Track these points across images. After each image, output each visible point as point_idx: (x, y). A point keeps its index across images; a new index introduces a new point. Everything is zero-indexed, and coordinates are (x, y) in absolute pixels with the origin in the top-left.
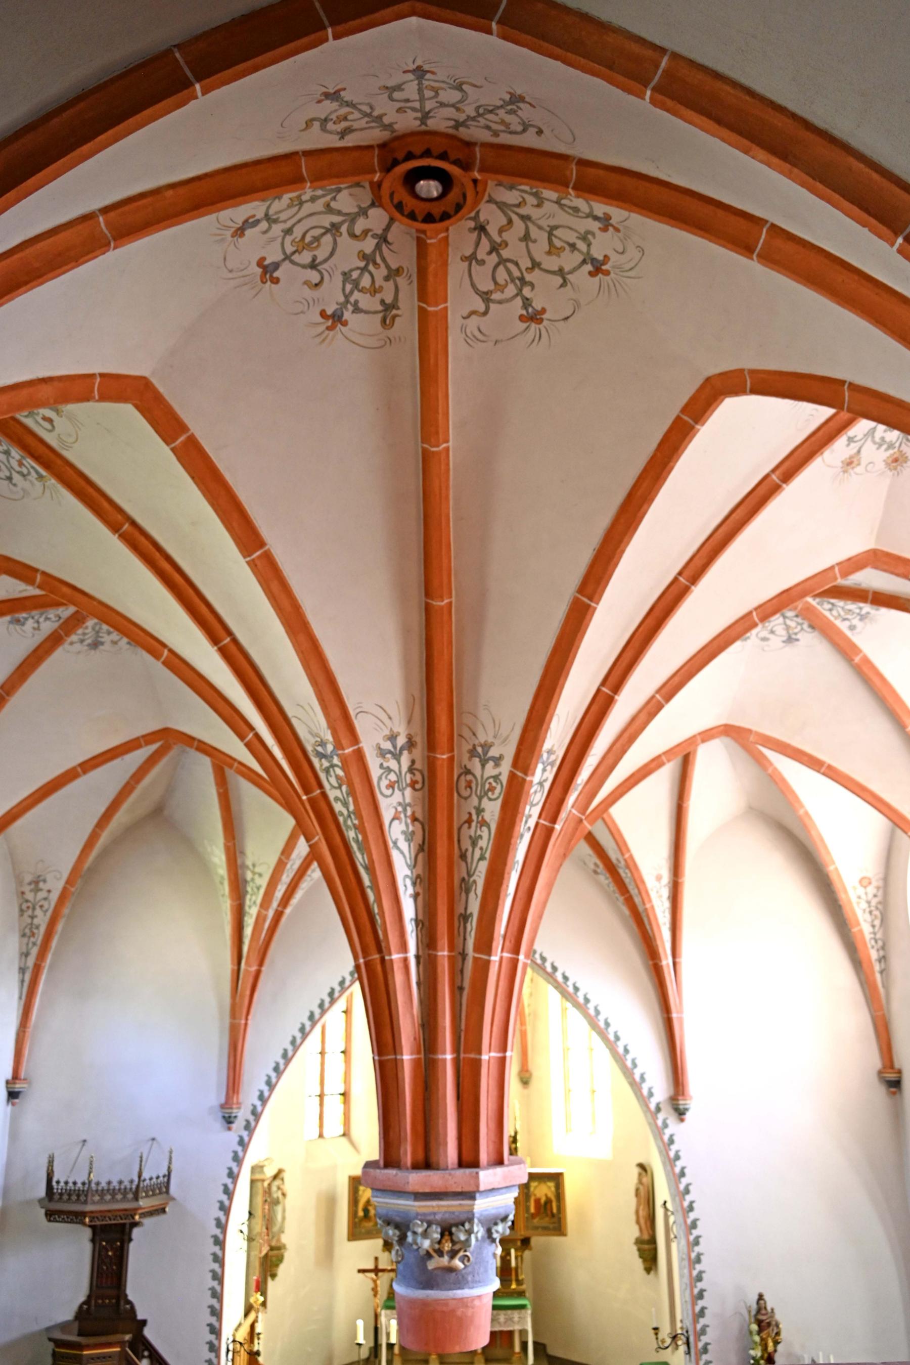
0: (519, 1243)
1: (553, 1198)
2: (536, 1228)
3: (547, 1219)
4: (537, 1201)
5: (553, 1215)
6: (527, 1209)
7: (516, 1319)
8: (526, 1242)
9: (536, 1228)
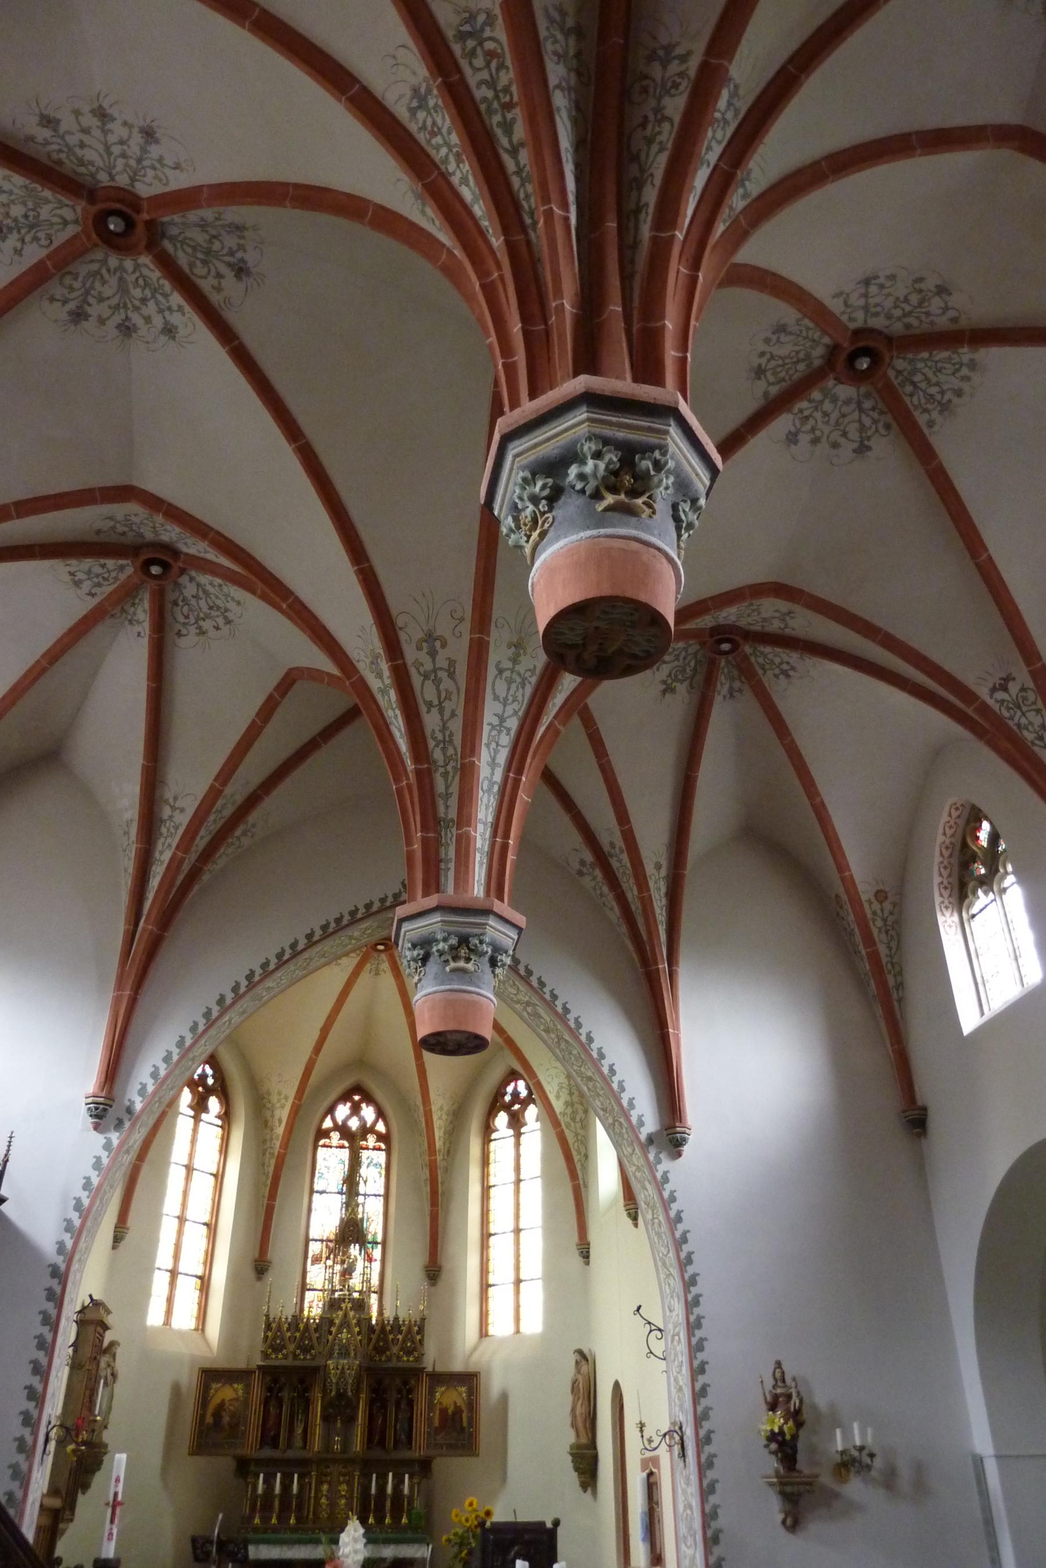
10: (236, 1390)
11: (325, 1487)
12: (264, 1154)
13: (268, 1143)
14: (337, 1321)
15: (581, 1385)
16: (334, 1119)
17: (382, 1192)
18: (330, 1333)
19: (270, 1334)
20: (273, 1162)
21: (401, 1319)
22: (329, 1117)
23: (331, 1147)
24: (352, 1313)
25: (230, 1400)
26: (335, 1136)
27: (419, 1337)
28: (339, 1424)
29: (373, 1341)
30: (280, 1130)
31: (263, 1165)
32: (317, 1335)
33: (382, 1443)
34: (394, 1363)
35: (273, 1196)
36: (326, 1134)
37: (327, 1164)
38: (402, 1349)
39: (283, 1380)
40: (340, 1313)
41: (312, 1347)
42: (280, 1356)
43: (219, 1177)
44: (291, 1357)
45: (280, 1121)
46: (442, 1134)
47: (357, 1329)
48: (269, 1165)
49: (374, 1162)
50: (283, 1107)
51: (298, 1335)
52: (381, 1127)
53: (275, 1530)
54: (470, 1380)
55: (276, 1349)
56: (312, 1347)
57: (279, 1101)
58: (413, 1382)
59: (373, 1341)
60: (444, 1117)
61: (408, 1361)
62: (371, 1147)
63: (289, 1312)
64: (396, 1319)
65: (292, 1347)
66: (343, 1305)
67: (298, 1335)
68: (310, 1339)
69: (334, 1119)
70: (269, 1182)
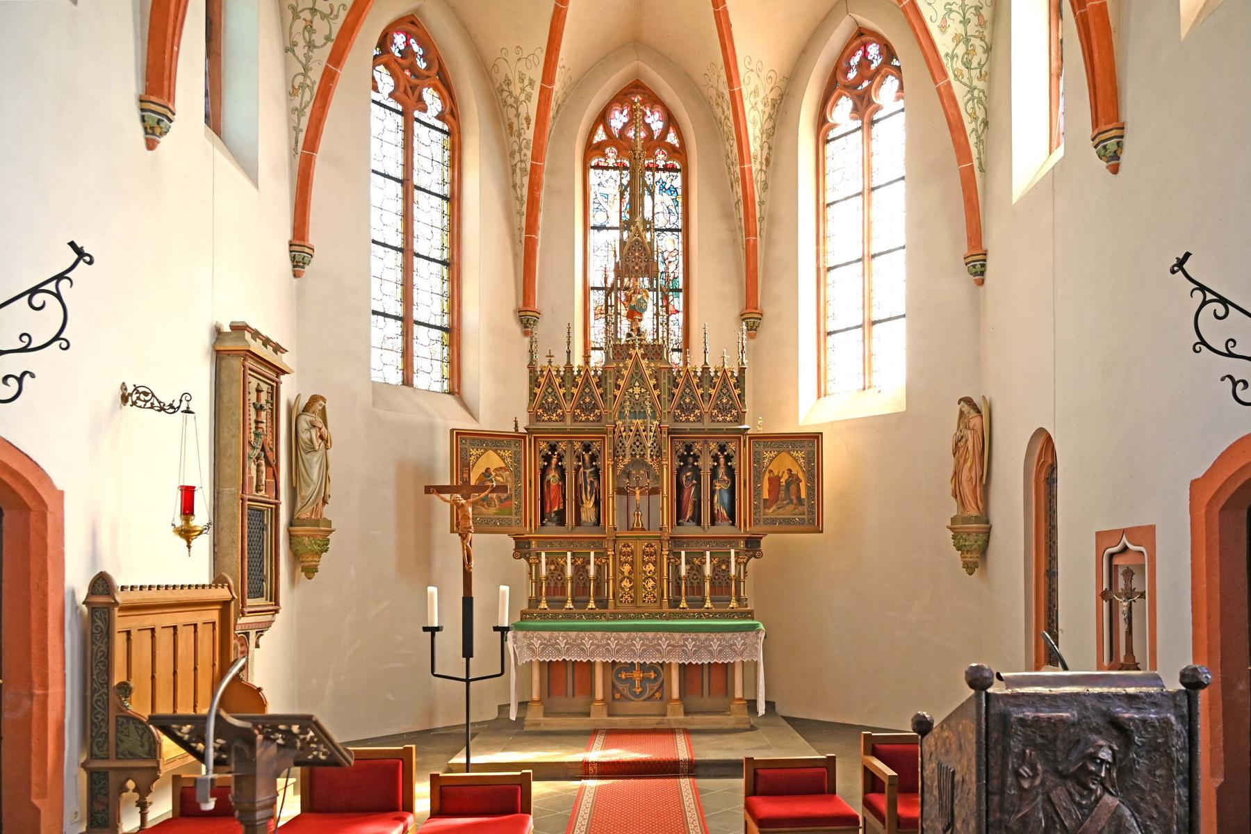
0: (742, 545)
3: (790, 507)
6: (758, 491)
8: (753, 544)
9: (773, 521)
11: (627, 568)
12: (514, 172)
13: (517, 155)
15: (970, 444)
16: (608, 130)
17: (680, 224)
18: (618, 387)
19: (537, 391)
20: (526, 180)
21: (712, 370)
22: (601, 127)
23: (607, 168)
24: (644, 362)
25: (496, 470)
26: (611, 152)
28: (638, 497)
30: (529, 134)
31: (514, 186)
33: (697, 519)
34: (707, 424)
35: (531, 227)
36: (599, 149)
37: (602, 190)
39: (562, 446)
40: (629, 362)
41: (596, 406)
42: (554, 417)
43: (453, 199)
44: (569, 419)
45: (528, 120)
46: (758, 134)
47: (652, 382)
48: (522, 185)
50: (529, 97)
51: (575, 391)
52: (672, 138)
53: (569, 616)
55: (549, 409)
56: (596, 406)
57: (523, 90)
58: (732, 447)
60: (760, 106)
61: (724, 421)
63: (560, 362)
64: (705, 369)
65: (568, 406)
66: (632, 352)
67: (575, 391)
69: (608, 130)
70: (524, 209)
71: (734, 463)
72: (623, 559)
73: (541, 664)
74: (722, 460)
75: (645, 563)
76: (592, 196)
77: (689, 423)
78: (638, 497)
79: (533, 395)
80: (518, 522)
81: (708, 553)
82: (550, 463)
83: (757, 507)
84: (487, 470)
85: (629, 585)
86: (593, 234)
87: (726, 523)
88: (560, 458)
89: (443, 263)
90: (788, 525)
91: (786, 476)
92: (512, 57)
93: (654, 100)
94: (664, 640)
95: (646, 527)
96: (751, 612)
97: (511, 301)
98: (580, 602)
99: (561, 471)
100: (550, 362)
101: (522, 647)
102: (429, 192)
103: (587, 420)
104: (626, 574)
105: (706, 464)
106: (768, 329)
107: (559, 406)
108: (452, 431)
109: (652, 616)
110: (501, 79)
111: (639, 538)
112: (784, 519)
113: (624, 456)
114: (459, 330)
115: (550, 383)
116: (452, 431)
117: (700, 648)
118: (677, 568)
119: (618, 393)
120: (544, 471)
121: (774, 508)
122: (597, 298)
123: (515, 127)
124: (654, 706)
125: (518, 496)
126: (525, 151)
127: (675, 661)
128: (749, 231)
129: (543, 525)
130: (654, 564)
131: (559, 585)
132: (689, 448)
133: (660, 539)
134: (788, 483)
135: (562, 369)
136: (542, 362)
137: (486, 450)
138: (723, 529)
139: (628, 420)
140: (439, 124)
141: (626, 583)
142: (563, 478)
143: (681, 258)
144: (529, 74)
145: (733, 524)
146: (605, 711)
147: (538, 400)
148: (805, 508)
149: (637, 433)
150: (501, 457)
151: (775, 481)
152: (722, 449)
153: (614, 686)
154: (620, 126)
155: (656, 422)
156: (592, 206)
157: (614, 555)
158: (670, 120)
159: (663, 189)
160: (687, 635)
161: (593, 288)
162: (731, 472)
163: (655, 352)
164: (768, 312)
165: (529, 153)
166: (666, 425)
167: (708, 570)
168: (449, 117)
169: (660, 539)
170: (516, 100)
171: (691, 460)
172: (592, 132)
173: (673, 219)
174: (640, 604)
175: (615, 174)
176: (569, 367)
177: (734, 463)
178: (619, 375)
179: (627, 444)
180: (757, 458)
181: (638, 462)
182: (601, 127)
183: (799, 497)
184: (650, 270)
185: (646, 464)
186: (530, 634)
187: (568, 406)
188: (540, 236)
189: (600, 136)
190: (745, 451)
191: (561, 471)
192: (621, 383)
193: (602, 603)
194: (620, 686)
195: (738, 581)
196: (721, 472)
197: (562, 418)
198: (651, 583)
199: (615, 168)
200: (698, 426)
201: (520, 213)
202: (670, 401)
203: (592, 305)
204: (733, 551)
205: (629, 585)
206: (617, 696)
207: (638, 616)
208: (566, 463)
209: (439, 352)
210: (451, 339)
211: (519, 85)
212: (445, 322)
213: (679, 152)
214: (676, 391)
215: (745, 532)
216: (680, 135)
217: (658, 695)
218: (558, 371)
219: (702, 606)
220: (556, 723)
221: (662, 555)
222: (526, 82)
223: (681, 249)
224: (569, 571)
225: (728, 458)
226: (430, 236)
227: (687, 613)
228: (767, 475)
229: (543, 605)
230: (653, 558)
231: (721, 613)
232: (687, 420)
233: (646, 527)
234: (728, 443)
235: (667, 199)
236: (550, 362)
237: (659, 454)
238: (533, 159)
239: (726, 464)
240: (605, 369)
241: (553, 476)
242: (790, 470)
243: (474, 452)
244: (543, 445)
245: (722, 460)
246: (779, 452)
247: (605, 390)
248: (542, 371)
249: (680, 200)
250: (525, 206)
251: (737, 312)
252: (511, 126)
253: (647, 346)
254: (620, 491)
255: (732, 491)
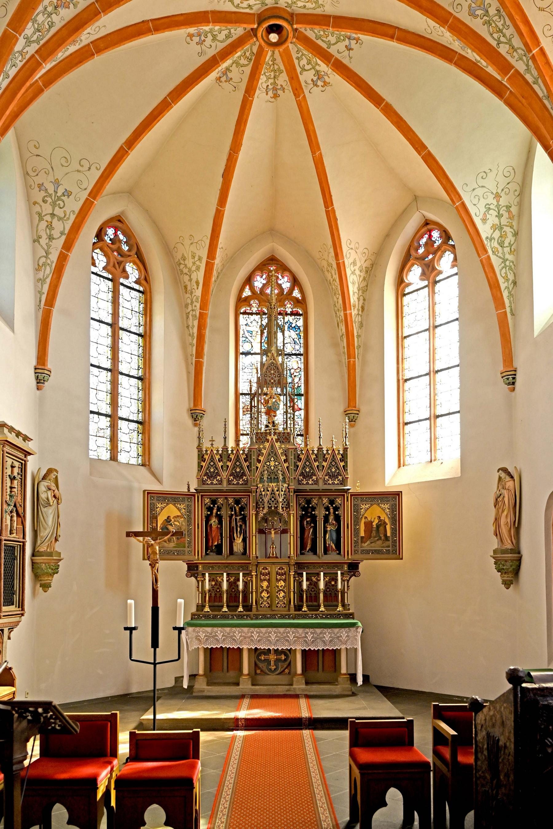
0: (346, 568)
1: (387, 521)
2: (367, 552)
4: (368, 525)
5: (387, 538)
6: (357, 531)
7: (344, 638)
8: (353, 568)
9: (367, 552)
10: (179, 510)
11: (265, 584)
12: (188, 317)
13: (190, 308)
14: (264, 452)
16: (252, 289)
17: (302, 351)
18: (259, 461)
19: (203, 464)
20: (196, 323)
22: (248, 287)
23: (252, 314)
24: (277, 445)
27: (342, 464)
28: (273, 535)
29: (300, 468)
30: (198, 292)
31: (188, 327)
32: (247, 464)
33: (314, 550)
34: (321, 486)
35: (199, 353)
36: (247, 300)
37: (248, 328)
38: (328, 474)
39: (220, 501)
40: (267, 445)
41: (244, 474)
44: (225, 483)
45: (197, 283)
47: (283, 458)
48: (193, 326)
49: (293, 326)
50: (198, 268)
51: (229, 464)
52: (296, 293)
54: (395, 497)
55: (211, 476)
56: (244, 474)
57: (194, 263)
58: (339, 501)
59: (300, 468)
61: (333, 484)
62: (289, 312)
63: (219, 445)
64: (320, 449)
65: (224, 474)
66: (269, 438)
67: (229, 464)
68: (242, 468)
69: (252, 289)
70: (195, 341)
71: (340, 512)
72: (262, 577)
73: (206, 649)
74: (332, 511)
75: (278, 580)
76: (241, 333)
77: (309, 485)
78: (273, 535)
79: (200, 467)
80: (189, 553)
81: (322, 574)
82: (212, 513)
83: (356, 542)
84: (168, 517)
85: (266, 595)
86: (242, 358)
87: (335, 553)
88: (219, 509)
89: (139, 378)
90: (378, 554)
91: (376, 521)
92: (187, 242)
93: (284, 268)
94: (291, 633)
95: (278, 555)
96: (352, 614)
97: (186, 404)
98: (232, 607)
99: (220, 518)
100: (212, 445)
101: (192, 638)
102: (130, 332)
103: (238, 484)
104: (265, 588)
105: (320, 513)
106: (362, 420)
107: (218, 474)
108: (144, 491)
109: (283, 617)
110: (179, 256)
111: (274, 563)
112: (375, 551)
113: (263, 508)
114: (149, 423)
115: (212, 459)
116: (144, 491)
117: (316, 639)
118: (300, 584)
119: (259, 465)
120: (208, 518)
121: (368, 542)
122: (244, 401)
123: (189, 288)
124: (284, 679)
125: (189, 535)
126: (195, 303)
127: (299, 647)
128: (350, 355)
129: (207, 554)
130: (284, 581)
131: (218, 595)
132: (309, 502)
133: (288, 564)
134: (378, 526)
135: (220, 449)
136: (206, 445)
137: (167, 504)
138: (332, 557)
139: (266, 484)
140: (137, 287)
141: (265, 594)
142: (220, 522)
143: (302, 373)
144: (198, 253)
145: (339, 554)
146: (250, 682)
147: (204, 470)
148: (390, 543)
149: (273, 492)
150: (178, 509)
151: (368, 525)
152: (332, 502)
153: (256, 665)
154: (260, 286)
155: (286, 485)
156: (241, 339)
157: (257, 575)
158: (295, 282)
159: (290, 327)
160: (307, 630)
161: (242, 394)
162: (337, 518)
163: (285, 437)
164: (364, 409)
165: (198, 305)
166: (292, 487)
167: (322, 585)
168: (144, 282)
169: (288, 564)
170: (190, 270)
171: (310, 510)
172: (242, 290)
173: (297, 347)
174: (274, 608)
175: (257, 318)
176: (225, 448)
177: (340, 512)
178: (260, 453)
179: (266, 500)
180: (356, 509)
181: (273, 512)
182: (248, 287)
183: (385, 535)
184: (281, 382)
185: (279, 513)
186: (197, 629)
187: (224, 474)
188: (205, 360)
189: (247, 292)
190: (348, 504)
191: (220, 518)
192: (261, 458)
193: (248, 608)
194: (261, 665)
195: (343, 593)
196: (331, 518)
197: (220, 482)
198: (282, 594)
199: (257, 314)
200: (315, 487)
201: (191, 344)
202: (295, 471)
203: (241, 405)
204: (339, 572)
205: (266, 595)
206: (258, 671)
207: (273, 617)
208: (223, 512)
209: (135, 437)
210: (144, 429)
211: (191, 261)
212: (140, 417)
213: (301, 302)
214: (299, 464)
215: (348, 559)
216: (302, 291)
217: (287, 671)
218: (218, 451)
219: (318, 610)
220: (216, 690)
221: (289, 575)
222: (196, 258)
223: (302, 368)
224: (225, 586)
225: (336, 509)
226: (130, 361)
227: (307, 615)
228: (363, 520)
229: (207, 609)
230: (283, 577)
231: (331, 615)
232: (308, 483)
233: (278, 555)
234: (335, 497)
235: (293, 334)
236: (212, 445)
237: (288, 506)
238: (200, 309)
239: (334, 513)
240: (250, 450)
241: (214, 521)
242: (379, 517)
243: (159, 505)
244: (207, 501)
245: (332, 511)
246: (372, 505)
247: (250, 463)
248: (206, 451)
249: (302, 335)
250: (195, 340)
251: (342, 409)
252: (186, 287)
253: (279, 433)
254: (261, 531)
255: (338, 531)
